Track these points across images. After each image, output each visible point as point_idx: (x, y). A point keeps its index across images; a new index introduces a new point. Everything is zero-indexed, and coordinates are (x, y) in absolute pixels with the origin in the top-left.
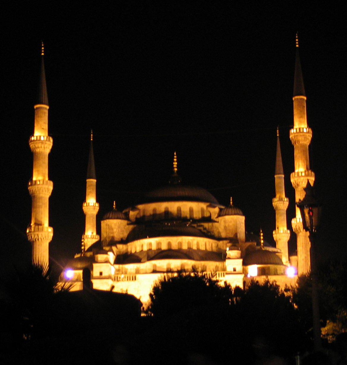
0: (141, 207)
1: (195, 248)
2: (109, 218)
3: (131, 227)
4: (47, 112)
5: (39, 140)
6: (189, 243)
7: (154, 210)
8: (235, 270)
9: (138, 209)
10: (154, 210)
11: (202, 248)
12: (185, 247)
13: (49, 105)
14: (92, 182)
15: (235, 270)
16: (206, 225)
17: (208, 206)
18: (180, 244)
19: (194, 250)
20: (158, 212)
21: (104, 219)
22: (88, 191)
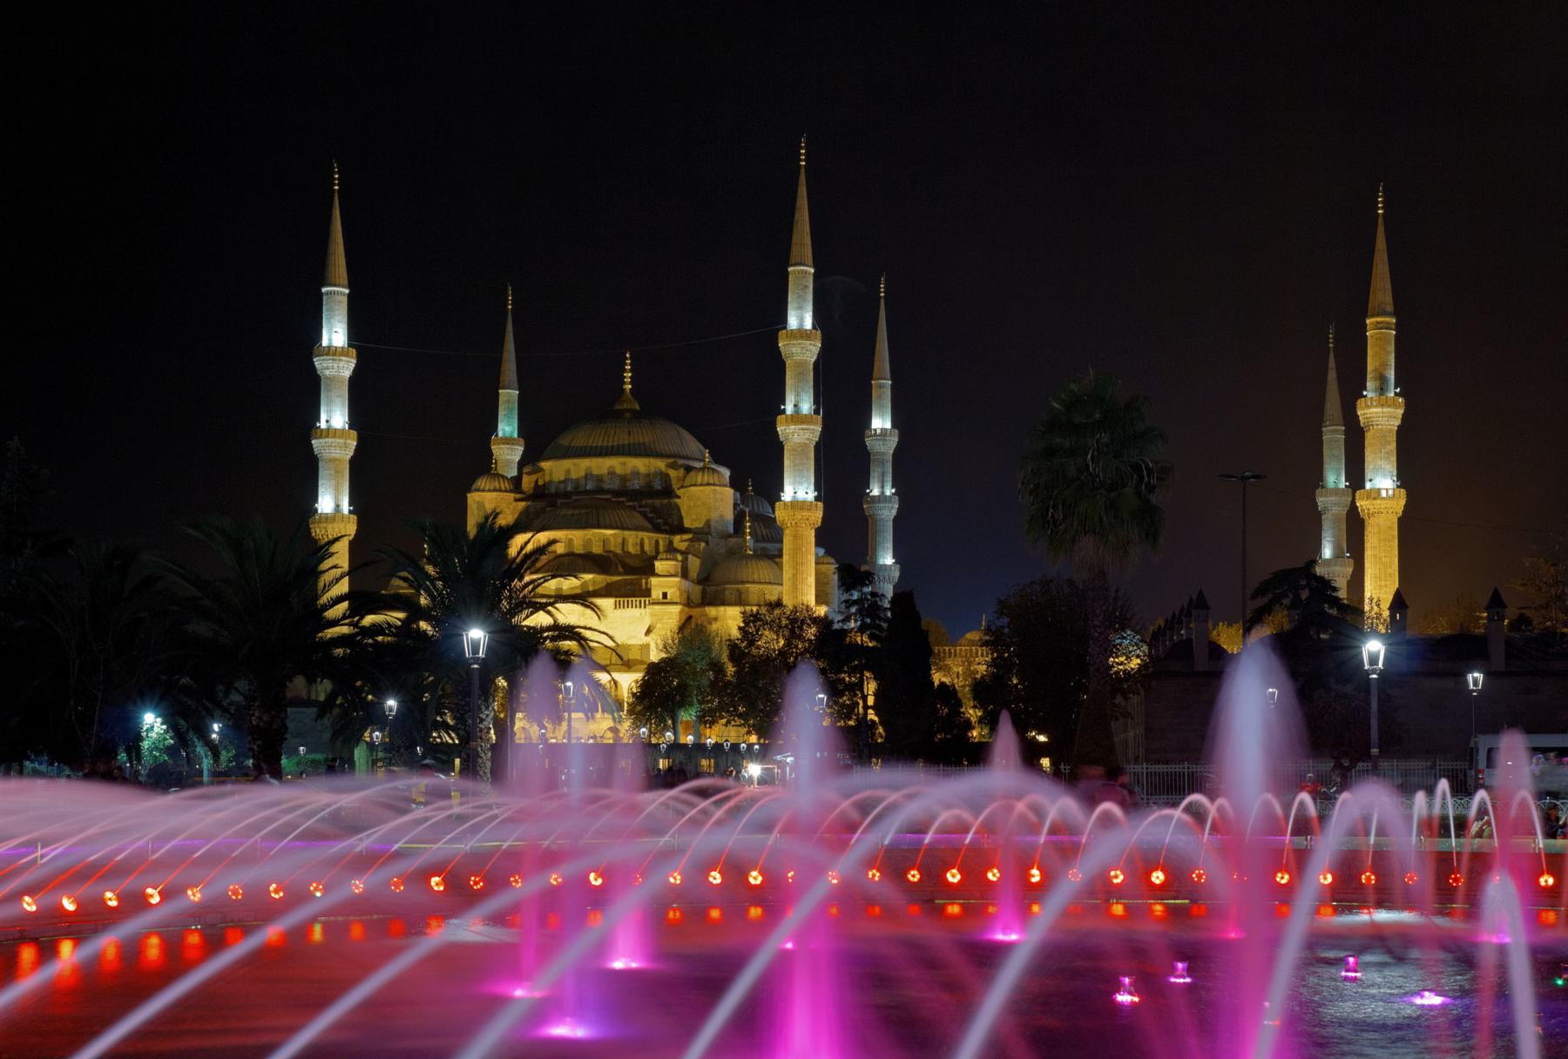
0: (545, 465)
1: (619, 551)
2: (478, 490)
3: (522, 505)
4: (345, 299)
5: (331, 351)
6: (605, 541)
7: (568, 472)
8: (665, 595)
9: (541, 470)
10: (568, 472)
11: (631, 549)
12: (597, 549)
13: (350, 287)
14: (509, 397)
15: (665, 595)
16: (657, 502)
17: (670, 466)
18: (588, 542)
19: (616, 555)
20: (574, 476)
21: (469, 491)
22: (501, 413)
